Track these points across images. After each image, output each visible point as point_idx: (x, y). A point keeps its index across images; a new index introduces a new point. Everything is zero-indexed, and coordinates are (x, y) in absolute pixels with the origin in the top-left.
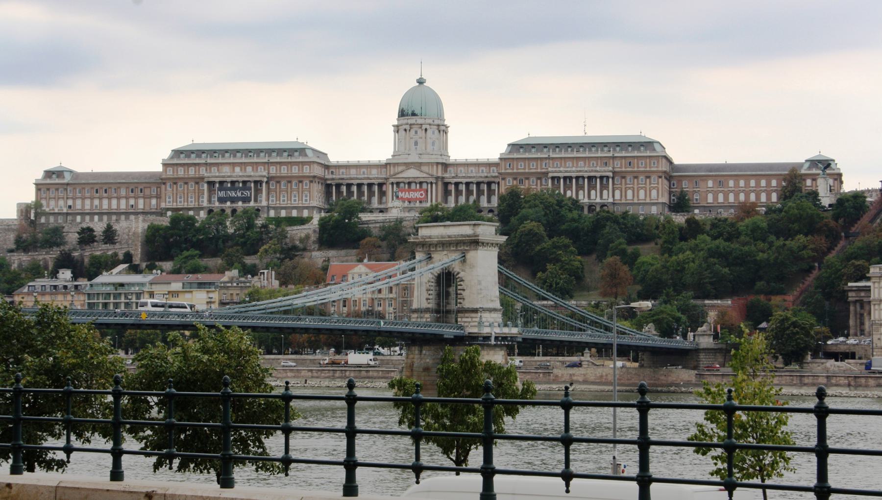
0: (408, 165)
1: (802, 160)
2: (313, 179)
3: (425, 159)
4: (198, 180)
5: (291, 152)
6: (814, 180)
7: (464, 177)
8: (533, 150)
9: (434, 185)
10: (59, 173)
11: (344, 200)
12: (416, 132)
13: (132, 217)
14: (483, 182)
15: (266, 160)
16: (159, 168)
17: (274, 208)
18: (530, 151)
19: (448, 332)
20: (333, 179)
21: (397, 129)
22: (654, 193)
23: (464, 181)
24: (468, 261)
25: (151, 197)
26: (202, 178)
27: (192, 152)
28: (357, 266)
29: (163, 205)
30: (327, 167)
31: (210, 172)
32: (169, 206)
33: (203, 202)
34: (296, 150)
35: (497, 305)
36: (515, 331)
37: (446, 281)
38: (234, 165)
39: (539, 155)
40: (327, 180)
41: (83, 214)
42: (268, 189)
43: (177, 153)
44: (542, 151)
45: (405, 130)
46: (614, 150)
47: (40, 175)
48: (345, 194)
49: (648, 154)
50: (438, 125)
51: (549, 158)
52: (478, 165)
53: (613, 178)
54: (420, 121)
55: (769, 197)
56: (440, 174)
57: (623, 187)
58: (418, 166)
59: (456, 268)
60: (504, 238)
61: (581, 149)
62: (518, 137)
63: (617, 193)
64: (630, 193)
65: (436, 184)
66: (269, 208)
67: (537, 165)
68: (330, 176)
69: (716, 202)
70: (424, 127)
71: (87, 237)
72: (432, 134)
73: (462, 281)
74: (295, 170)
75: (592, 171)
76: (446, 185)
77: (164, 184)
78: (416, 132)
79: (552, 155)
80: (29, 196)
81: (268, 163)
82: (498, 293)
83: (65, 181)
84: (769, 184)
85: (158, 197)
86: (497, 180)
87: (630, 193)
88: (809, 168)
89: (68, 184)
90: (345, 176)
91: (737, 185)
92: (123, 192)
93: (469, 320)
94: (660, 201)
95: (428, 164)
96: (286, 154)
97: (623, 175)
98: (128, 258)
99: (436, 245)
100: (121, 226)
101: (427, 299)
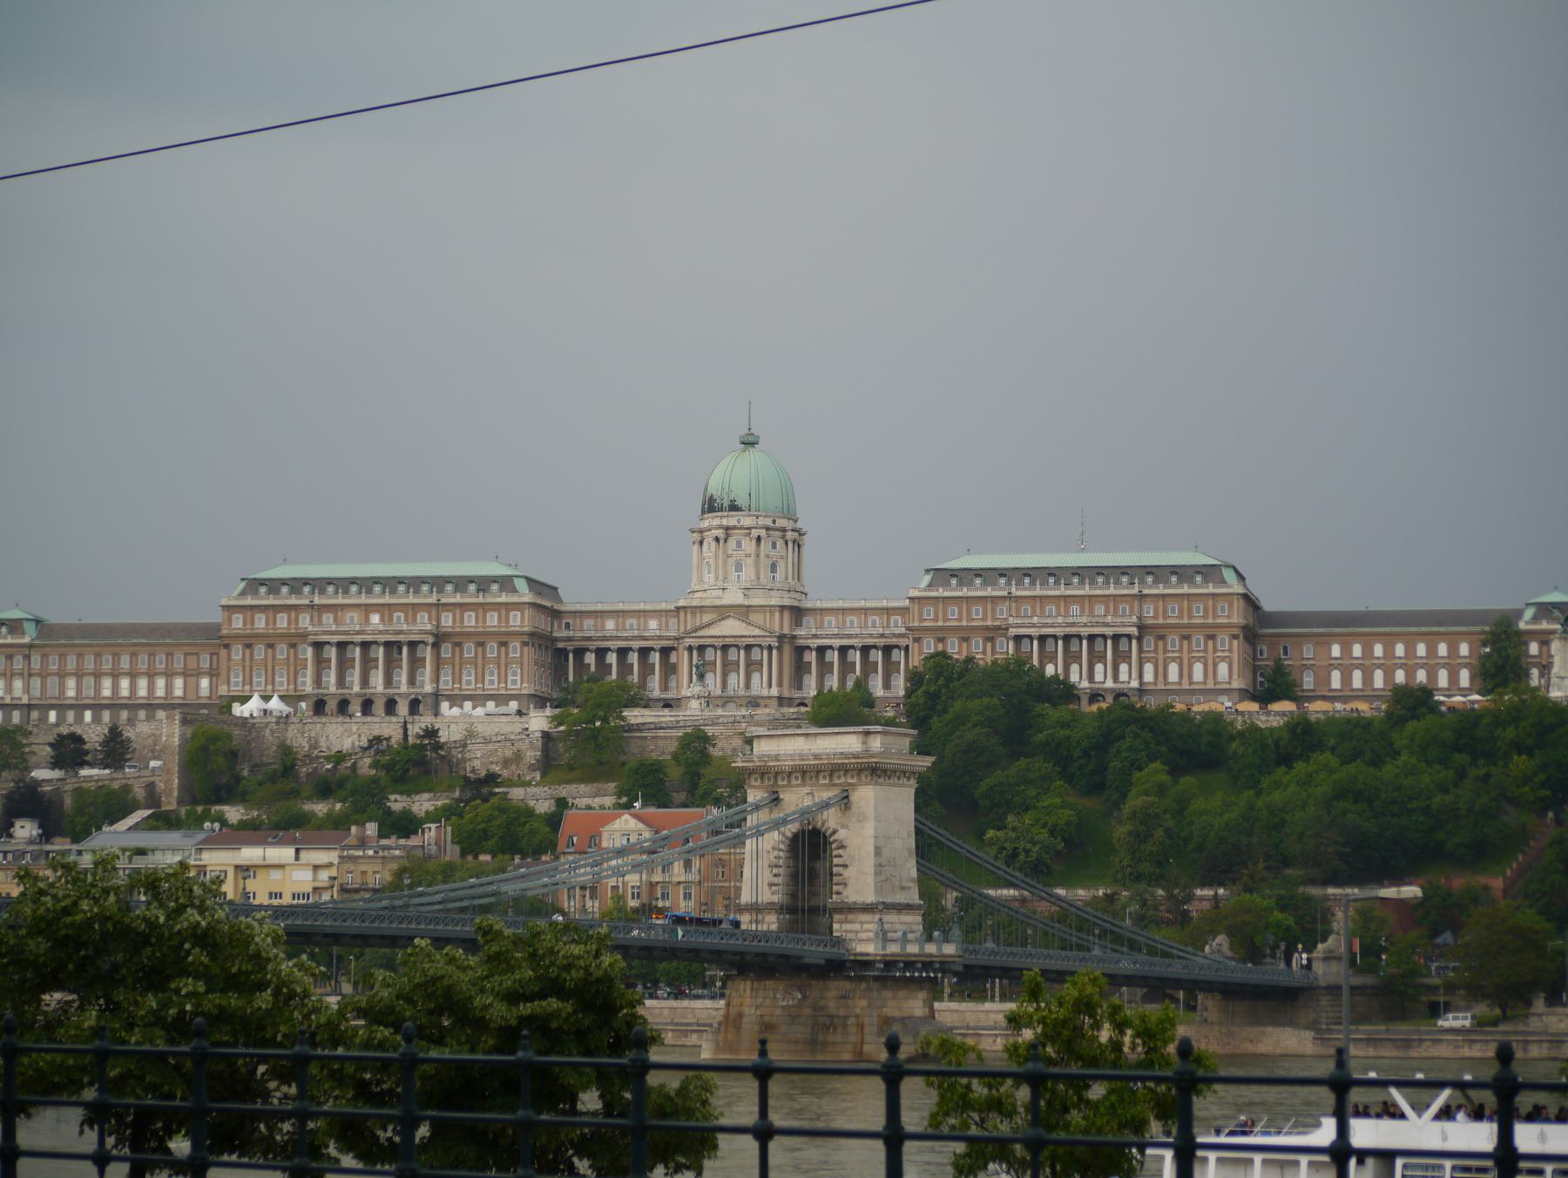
0: (723, 612)
3: (757, 600)
7: (836, 636)
8: (978, 581)
9: (775, 652)
11: (594, 679)
12: (739, 544)
13: (161, 714)
14: (875, 647)
15: (433, 599)
18: (970, 584)
19: (813, 951)
20: (570, 639)
22: (1223, 668)
23: (837, 643)
24: (854, 808)
25: (199, 674)
28: (620, 816)
29: (223, 690)
31: (320, 623)
33: (304, 683)
35: (914, 897)
36: (949, 949)
37: (810, 851)
38: (367, 609)
39: (989, 592)
40: (556, 640)
41: (61, 708)
44: (994, 584)
45: (717, 539)
46: (1142, 582)
48: (593, 669)
49: (1211, 589)
50: (784, 530)
51: (1009, 597)
53: (1140, 639)
54: (747, 521)
56: (786, 631)
57: (1161, 657)
58: (743, 612)
59: (830, 820)
60: (926, 762)
61: (1076, 580)
63: (1149, 668)
65: (779, 648)
67: (985, 613)
68: (564, 634)
70: (755, 533)
71: (69, 752)
73: (843, 847)
74: (492, 620)
77: (227, 646)
78: (739, 544)
79: (1015, 592)
82: (914, 873)
83: (26, 640)
85: (213, 673)
86: (903, 642)
88: (1535, 619)
89: (30, 646)
90: (593, 634)
93: (857, 927)
95: (761, 608)
96: (472, 587)
97: (1161, 632)
98: (153, 799)
99: (790, 774)
100: (139, 731)
101: (771, 885)
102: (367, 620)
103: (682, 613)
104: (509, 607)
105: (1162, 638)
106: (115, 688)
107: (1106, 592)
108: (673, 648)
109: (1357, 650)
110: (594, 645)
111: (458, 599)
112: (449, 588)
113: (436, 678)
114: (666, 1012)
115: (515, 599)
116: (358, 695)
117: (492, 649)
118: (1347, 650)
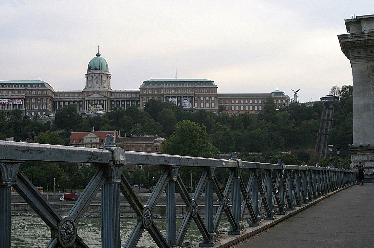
0: (94, 92)
2: (48, 97)
5: (37, 84)
6: (282, 100)
7: (120, 98)
9: (106, 102)
12: (97, 77)
20: (57, 99)
21: (87, 76)
22: (213, 104)
23: (120, 100)
30: (54, 93)
34: (40, 84)
45: (92, 76)
46: (194, 85)
50: (107, 74)
51: (164, 88)
52: (126, 93)
54: (99, 72)
56: (109, 97)
58: (99, 92)
62: (148, 79)
66: (26, 111)
68: (55, 98)
69: (235, 109)
72: (104, 78)
74: (39, 93)
75: (185, 94)
76: (111, 101)
78: (97, 77)
81: (26, 89)
84: (258, 102)
88: (275, 95)
94: (216, 108)
96: (34, 86)
97: (199, 96)
102: (9, 93)
103: (84, 93)
107: (186, 87)
108: (82, 101)
110: (62, 100)
111: (31, 88)
112: (29, 86)
113: (25, 107)
115: (45, 88)
116: (6, 111)
117: (39, 99)
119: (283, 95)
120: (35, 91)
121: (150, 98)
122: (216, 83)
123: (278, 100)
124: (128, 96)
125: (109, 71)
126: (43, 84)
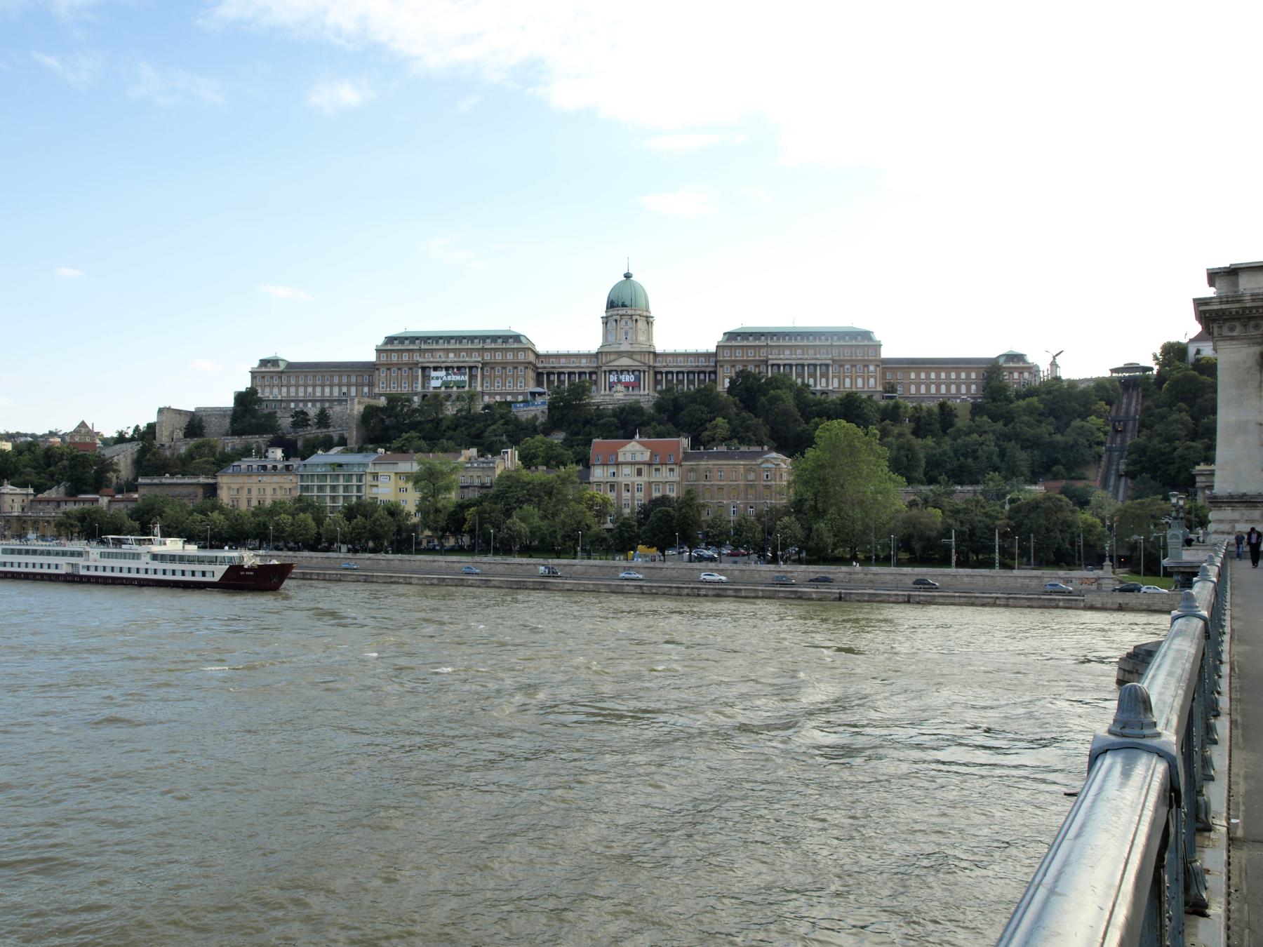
0: (620, 354)
1: (994, 356)
4: (412, 366)
5: (506, 338)
6: (1021, 373)
10: (275, 362)
16: (371, 357)
17: (489, 394)
21: (606, 320)
22: (872, 381)
23: (675, 370)
25: (363, 385)
26: (416, 364)
27: (406, 338)
29: (376, 390)
30: (537, 356)
32: (382, 391)
34: (511, 337)
38: (448, 351)
41: (297, 401)
42: (483, 374)
43: (390, 340)
47: (256, 364)
51: (767, 346)
52: (686, 355)
54: (630, 312)
55: (968, 389)
58: (630, 354)
64: (848, 381)
66: (483, 393)
69: (921, 393)
71: (301, 419)
74: (510, 356)
76: (656, 373)
80: (244, 384)
81: (482, 349)
87: (848, 381)
88: (1006, 361)
91: (958, 376)
92: (336, 380)
104: (518, 350)
105: (842, 366)
106: (323, 391)
108: (595, 373)
109: (923, 376)
110: (556, 371)
111: (493, 346)
114: (736, 573)
118: (918, 375)
119: (1025, 362)
120: (504, 349)
121: (739, 367)
122: (877, 336)
123: (1011, 373)
124: (691, 364)
125: (652, 308)
126: (517, 338)
